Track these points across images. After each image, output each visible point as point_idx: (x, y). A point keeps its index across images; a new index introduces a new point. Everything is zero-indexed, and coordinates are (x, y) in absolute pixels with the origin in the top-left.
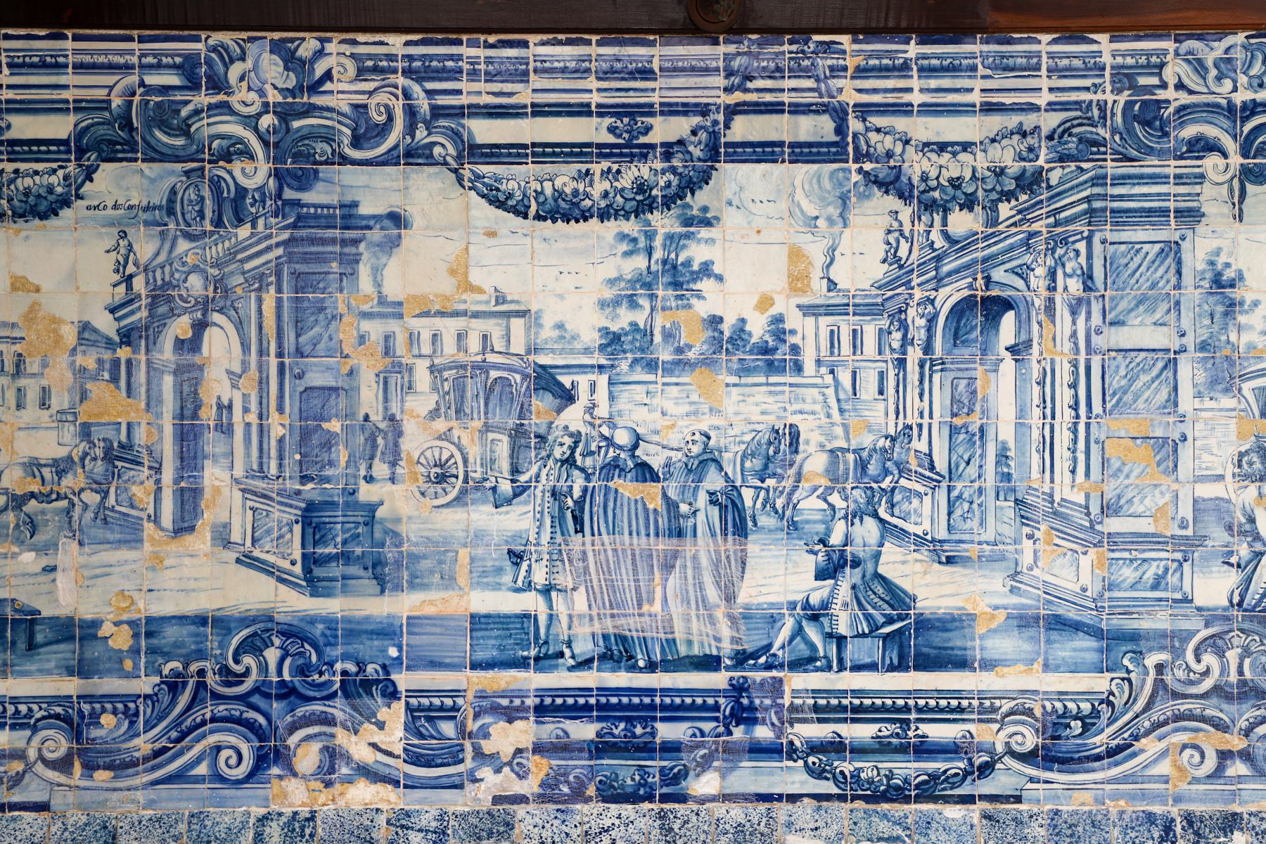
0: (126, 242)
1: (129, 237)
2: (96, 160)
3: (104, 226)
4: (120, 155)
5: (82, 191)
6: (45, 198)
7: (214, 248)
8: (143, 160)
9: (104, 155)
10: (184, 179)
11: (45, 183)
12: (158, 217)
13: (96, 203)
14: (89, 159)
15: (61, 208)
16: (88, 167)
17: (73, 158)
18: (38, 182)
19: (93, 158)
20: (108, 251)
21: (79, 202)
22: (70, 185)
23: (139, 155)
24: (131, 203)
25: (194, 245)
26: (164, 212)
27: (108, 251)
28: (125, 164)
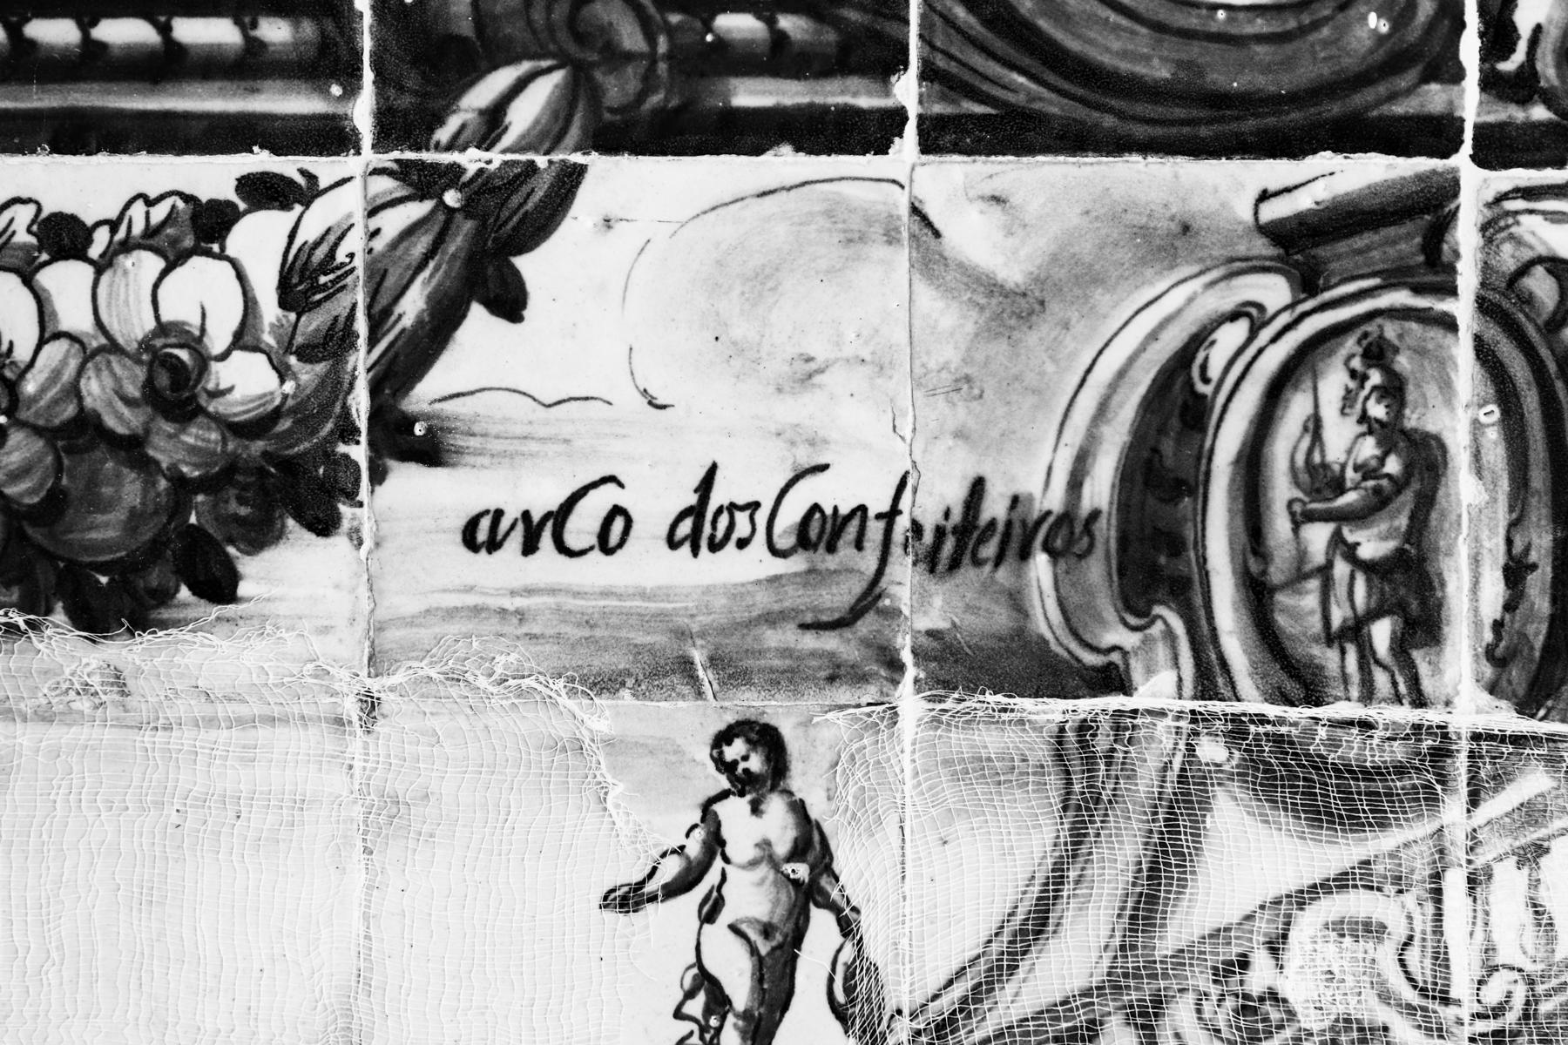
0: (777, 824)
1: (805, 780)
2: (549, 135)
3: (604, 684)
4: (750, 94)
5: (424, 394)
6: (132, 448)
7: (1509, 882)
8: (937, 136)
9: (617, 88)
10: (1273, 291)
11: (134, 324)
12: (1045, 618)
13: (544, 500)
14: (494, 117)
15: (261, 536)
16: (484, 190)
17: (362, 112)
18: (74, 315)
19: (524, 114)
20: (628, 899)
21: (406, 479)
22: (337, 341)
23: (907, 90)
24: (834, 493)
25: (1342, 852)
26: (1096, 571)
27: (628, 899)
28: (784, 163)
